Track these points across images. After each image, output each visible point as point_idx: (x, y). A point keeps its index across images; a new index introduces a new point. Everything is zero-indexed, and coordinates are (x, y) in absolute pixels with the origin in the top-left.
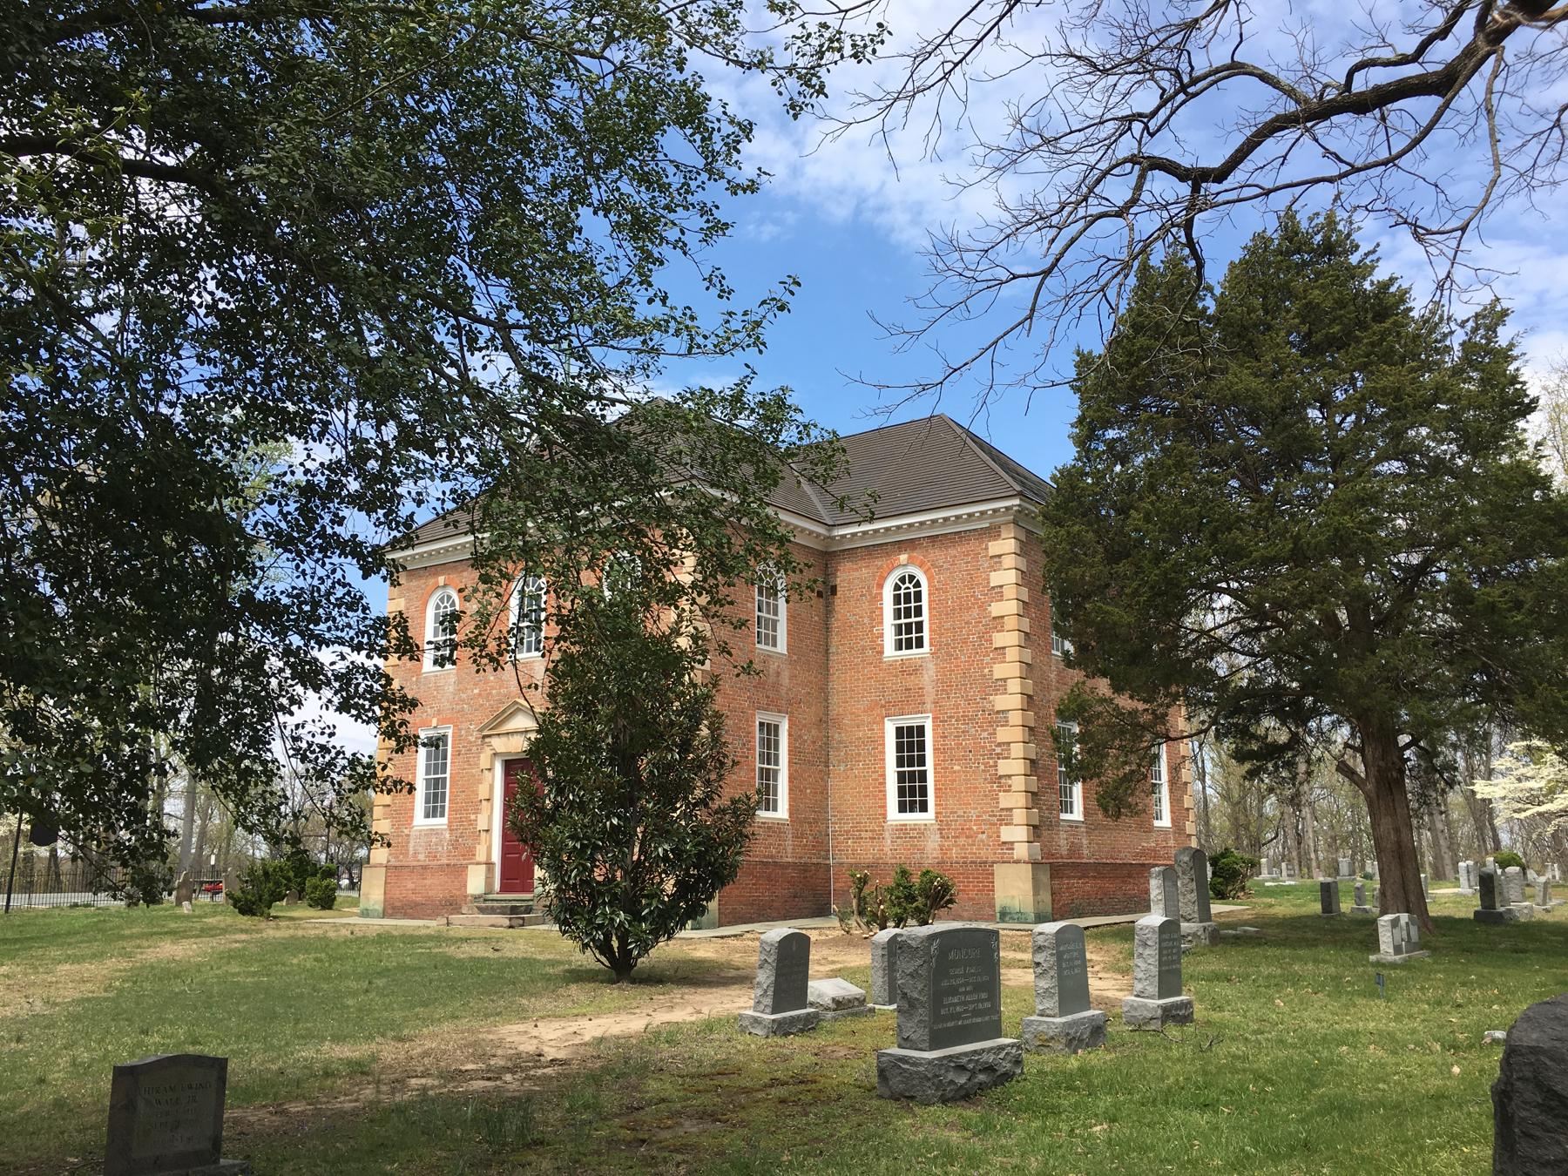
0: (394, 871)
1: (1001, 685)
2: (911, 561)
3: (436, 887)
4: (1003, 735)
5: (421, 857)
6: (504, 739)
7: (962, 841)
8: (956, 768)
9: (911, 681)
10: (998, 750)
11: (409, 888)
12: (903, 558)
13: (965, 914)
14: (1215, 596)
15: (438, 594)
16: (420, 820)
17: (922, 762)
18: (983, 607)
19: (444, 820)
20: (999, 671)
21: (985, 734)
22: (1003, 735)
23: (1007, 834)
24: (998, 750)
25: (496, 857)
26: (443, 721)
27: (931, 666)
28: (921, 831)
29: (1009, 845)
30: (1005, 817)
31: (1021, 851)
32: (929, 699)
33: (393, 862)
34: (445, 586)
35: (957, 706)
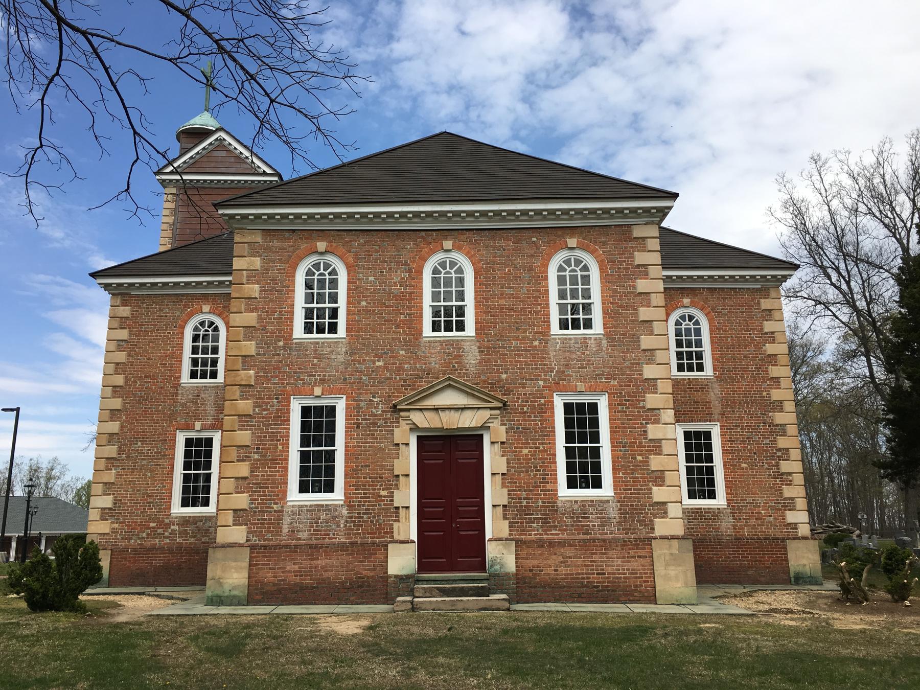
0: (259, 552)
1: (779, 406)
2: (693, 305)
3: (333, 567)
4: (782, 442)
5: (304, 535)
6: (428, 414)
7: (753, 522)
8: (744, 465)
9: (698, 396)
10: (779, 454)
11: (290, 569)
12: (686, 301)
13: (763, 579)
14: (863, 358)
15: (313, 259)
16: (294, 496)
17: (710, 459)
18: (759, 347)
19: (338, 496)
20: (776, 394)
21: (767, 441)
22: (782, 442)
23: (791, 517)
24: (779, 454)
25: (414, 536)
26: (329, 391)
27: (716, 386)
28: (716, 514)
29: (794, 526)
30: (790, 504)
31: (804, 530)
32: (716, 409)
33: (255, 540)
34: (326, 252)
35: (741, 418)
